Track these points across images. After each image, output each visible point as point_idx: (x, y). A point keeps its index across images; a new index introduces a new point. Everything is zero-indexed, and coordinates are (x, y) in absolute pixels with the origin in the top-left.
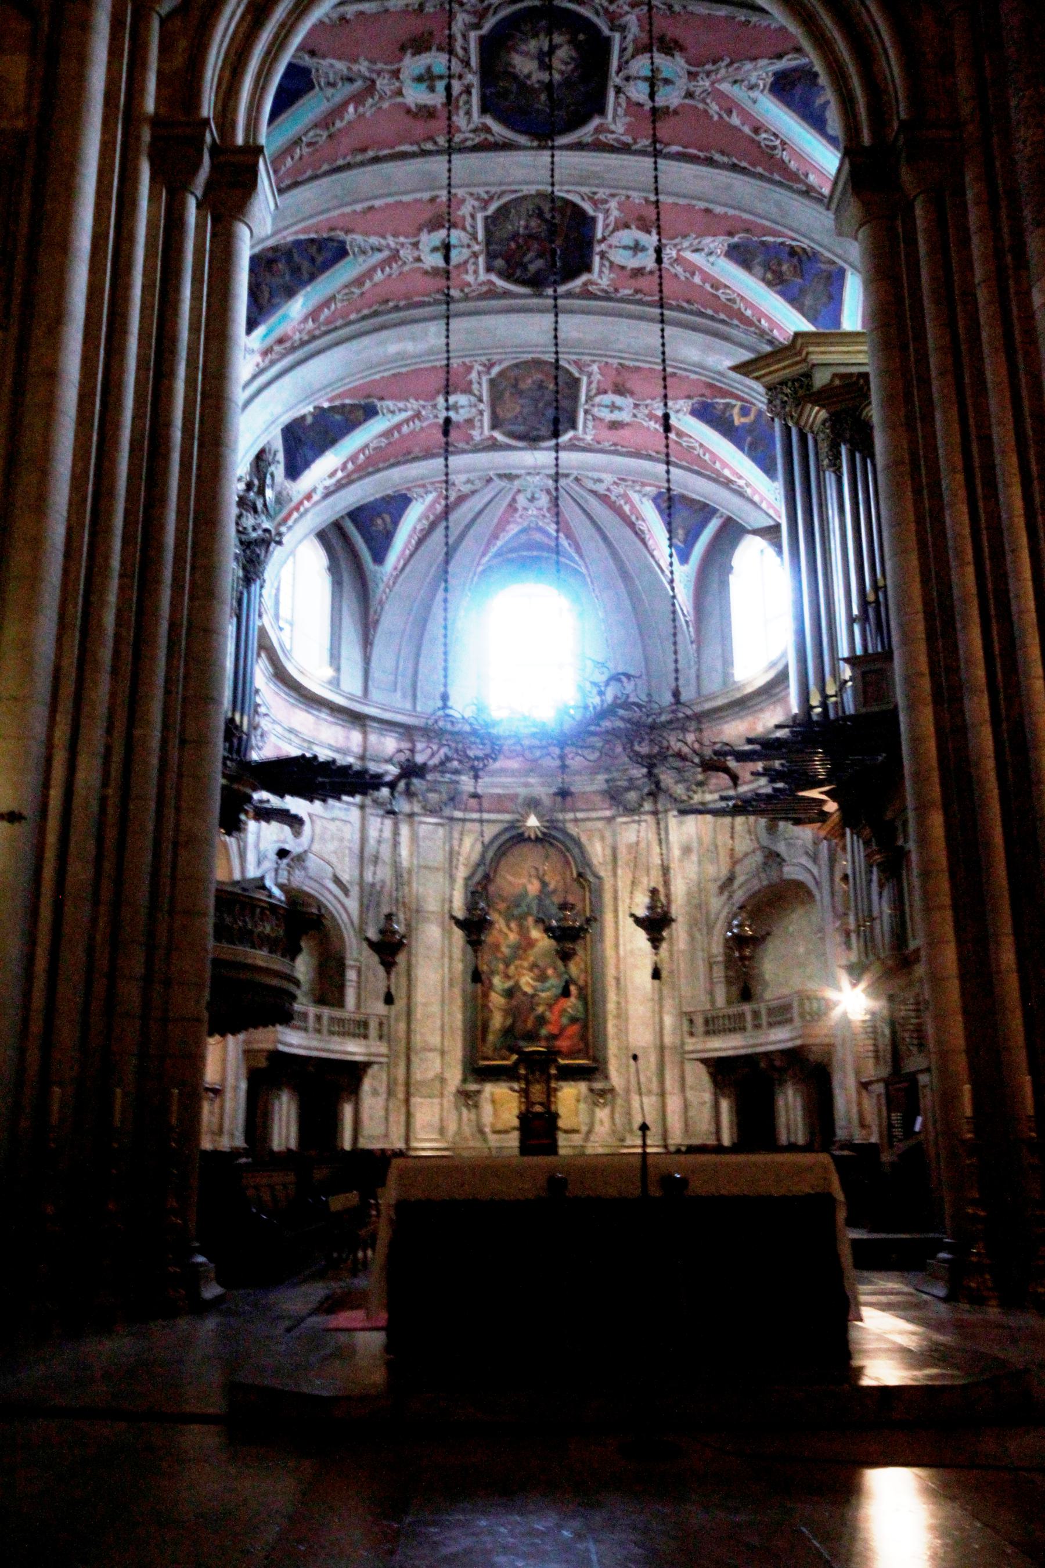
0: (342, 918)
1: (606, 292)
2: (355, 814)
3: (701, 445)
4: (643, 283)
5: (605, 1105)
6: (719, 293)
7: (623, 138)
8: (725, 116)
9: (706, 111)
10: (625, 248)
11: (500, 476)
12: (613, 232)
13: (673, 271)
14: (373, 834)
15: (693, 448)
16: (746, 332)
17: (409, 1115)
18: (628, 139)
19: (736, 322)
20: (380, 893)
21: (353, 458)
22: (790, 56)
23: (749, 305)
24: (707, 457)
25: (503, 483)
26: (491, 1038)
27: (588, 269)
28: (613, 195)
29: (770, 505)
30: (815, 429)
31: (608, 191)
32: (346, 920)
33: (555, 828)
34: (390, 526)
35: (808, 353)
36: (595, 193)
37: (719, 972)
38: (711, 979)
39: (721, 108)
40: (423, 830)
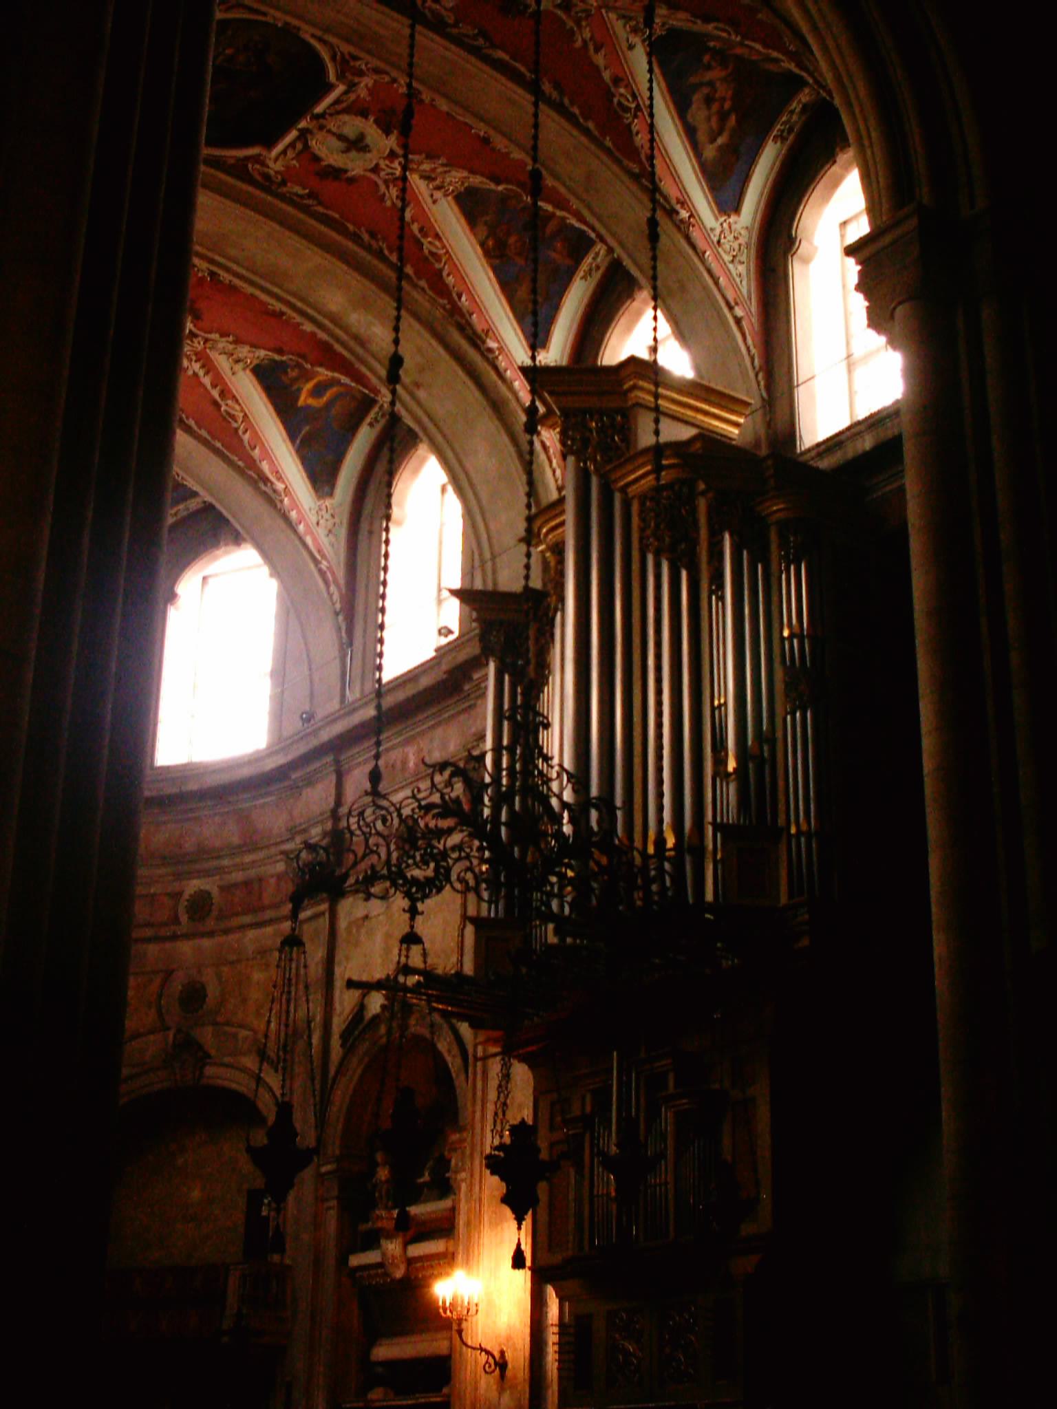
1: (267, 177)
3: (245, 415)
6: (423, 240)
7: (444, 12)
8: (591, 48)
9: (572, 33)
10: (341, 137)
12: (338, 113)
13: (383, 188)
15: (233, 417)
16: (433, 302)
18: (450, 19)
19: (423, 283)
22: (721, 25)
23: (456, 270)
24: (246, 437)
27: (270, 144)
28: (377, 71)
29: (309, 530)
30: (632, 490)
31: (376, 63)
35: (635, 387)
36: (356, 58)
39: (591, 39)
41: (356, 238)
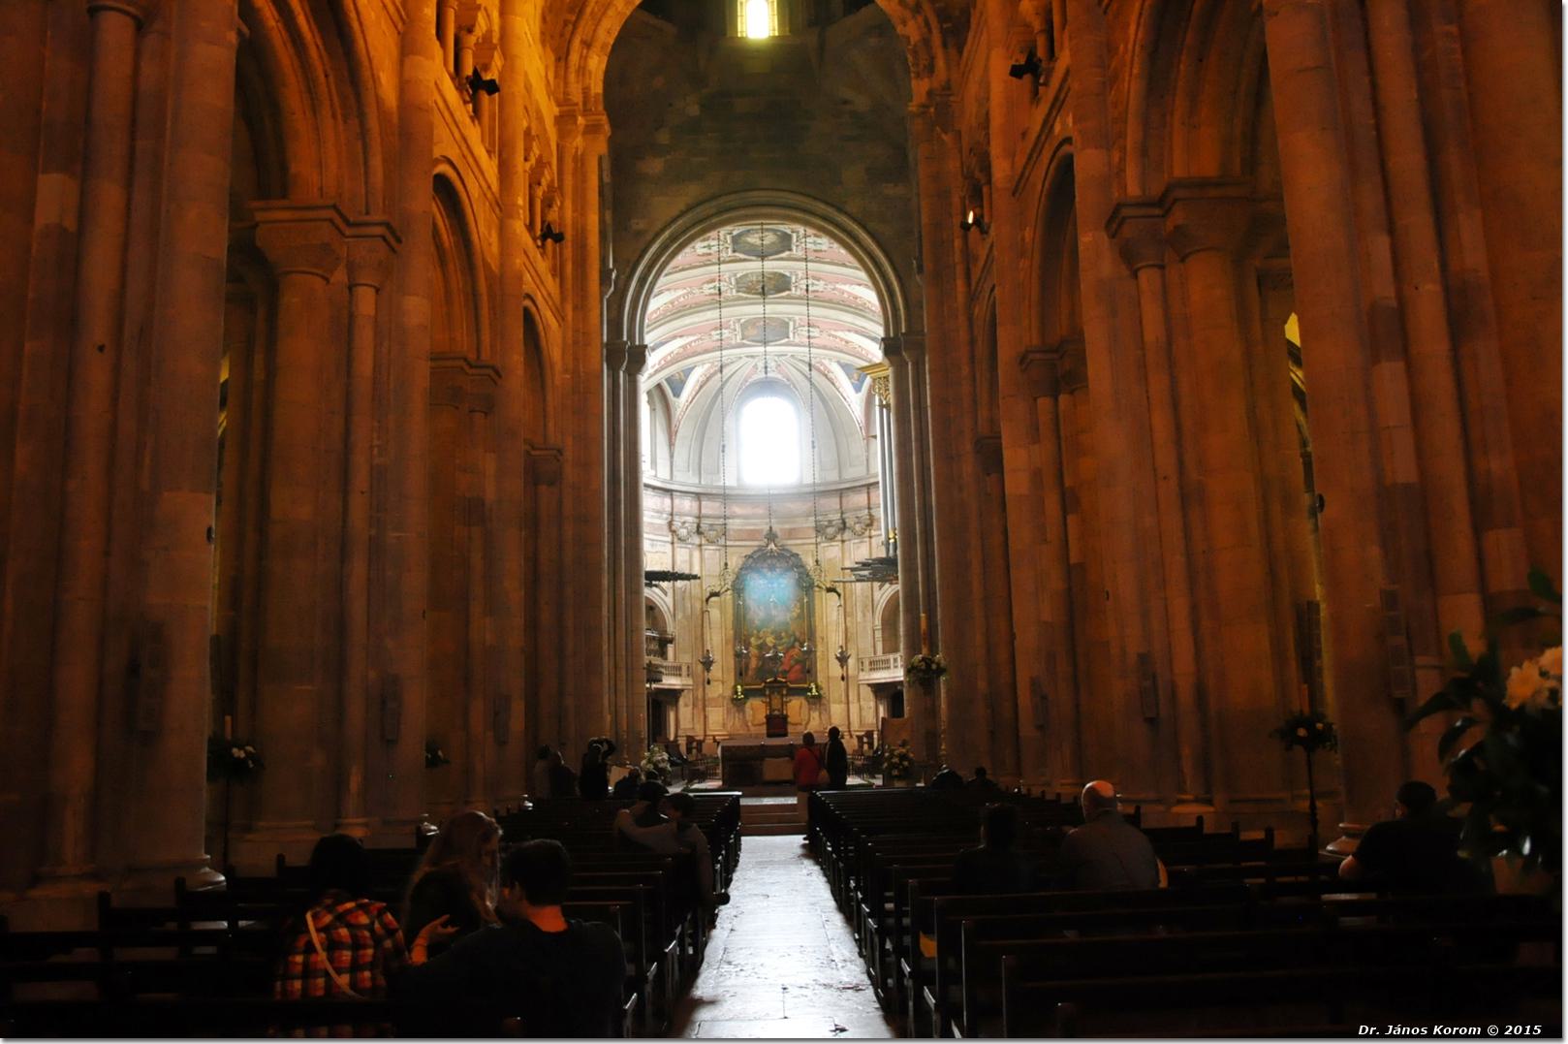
0: (664, 609)
2: (669, 546)
4: (816, 294)
5: (816, 709)
11: (747, 357)
14: (679, 559)
17: (705, 717)
20: (685, 592)
21: (664, 358)
25: (750, 359)
26: (750, 673)
27: (790, 290)
32: (666, 608)
33: (784, 550)
34: (683, 377)
37: (879, 634)
38: (874, 638)
40: (706, 554)
41: (839, 304)
